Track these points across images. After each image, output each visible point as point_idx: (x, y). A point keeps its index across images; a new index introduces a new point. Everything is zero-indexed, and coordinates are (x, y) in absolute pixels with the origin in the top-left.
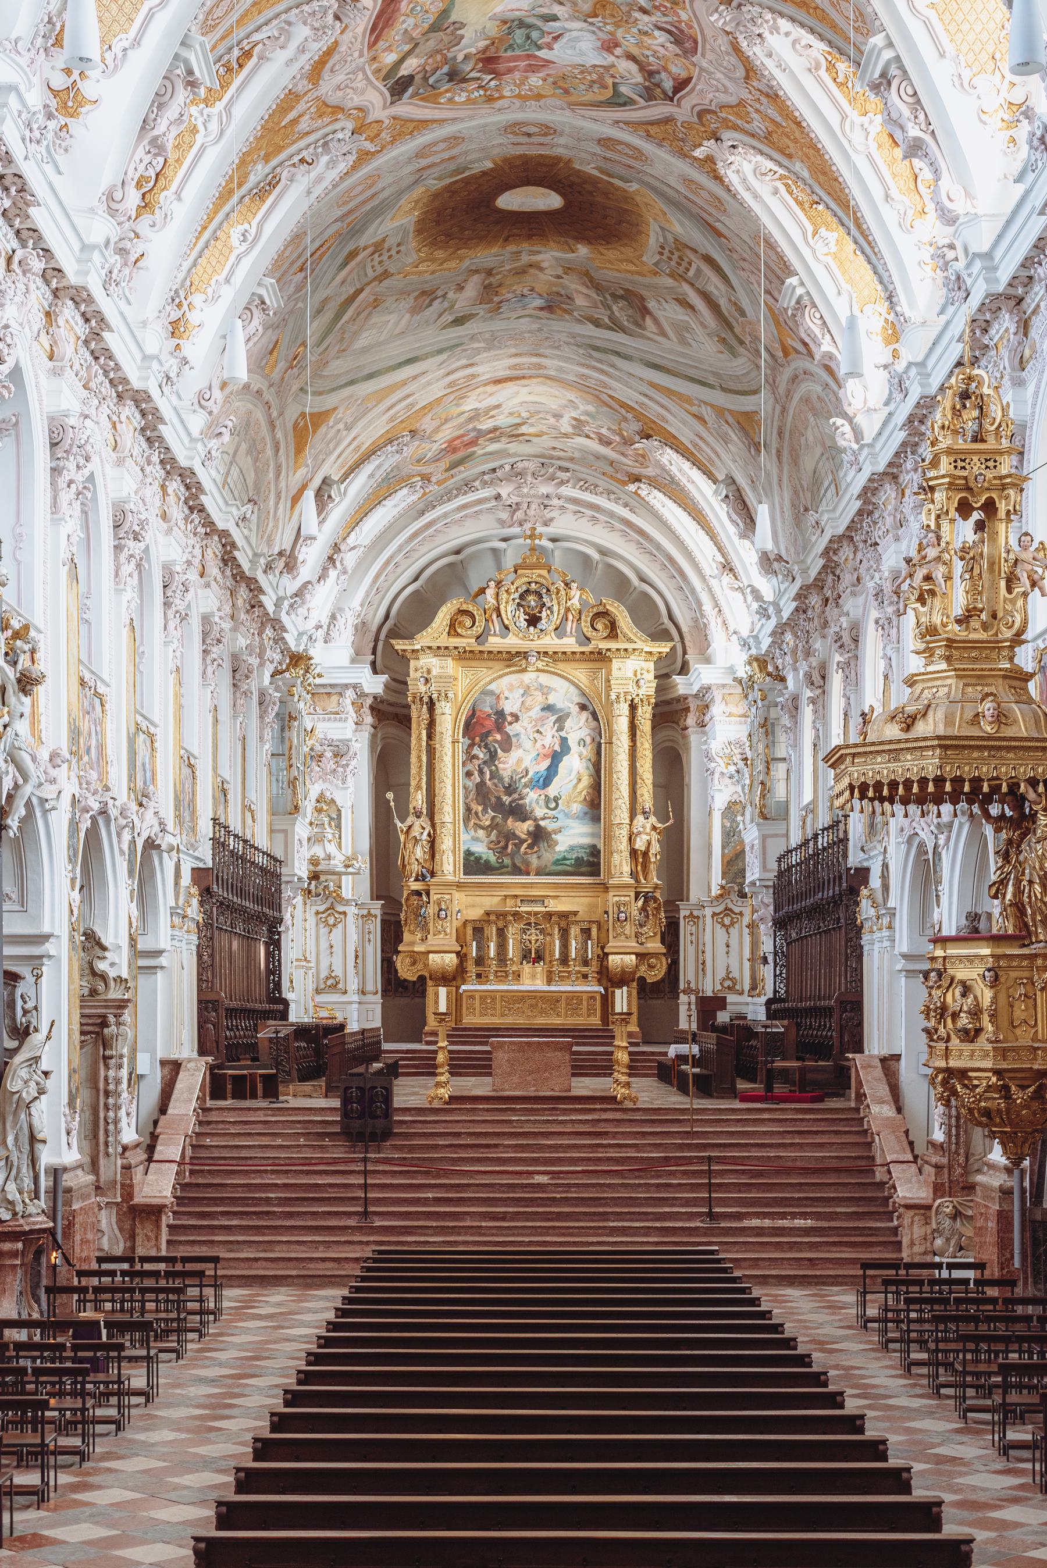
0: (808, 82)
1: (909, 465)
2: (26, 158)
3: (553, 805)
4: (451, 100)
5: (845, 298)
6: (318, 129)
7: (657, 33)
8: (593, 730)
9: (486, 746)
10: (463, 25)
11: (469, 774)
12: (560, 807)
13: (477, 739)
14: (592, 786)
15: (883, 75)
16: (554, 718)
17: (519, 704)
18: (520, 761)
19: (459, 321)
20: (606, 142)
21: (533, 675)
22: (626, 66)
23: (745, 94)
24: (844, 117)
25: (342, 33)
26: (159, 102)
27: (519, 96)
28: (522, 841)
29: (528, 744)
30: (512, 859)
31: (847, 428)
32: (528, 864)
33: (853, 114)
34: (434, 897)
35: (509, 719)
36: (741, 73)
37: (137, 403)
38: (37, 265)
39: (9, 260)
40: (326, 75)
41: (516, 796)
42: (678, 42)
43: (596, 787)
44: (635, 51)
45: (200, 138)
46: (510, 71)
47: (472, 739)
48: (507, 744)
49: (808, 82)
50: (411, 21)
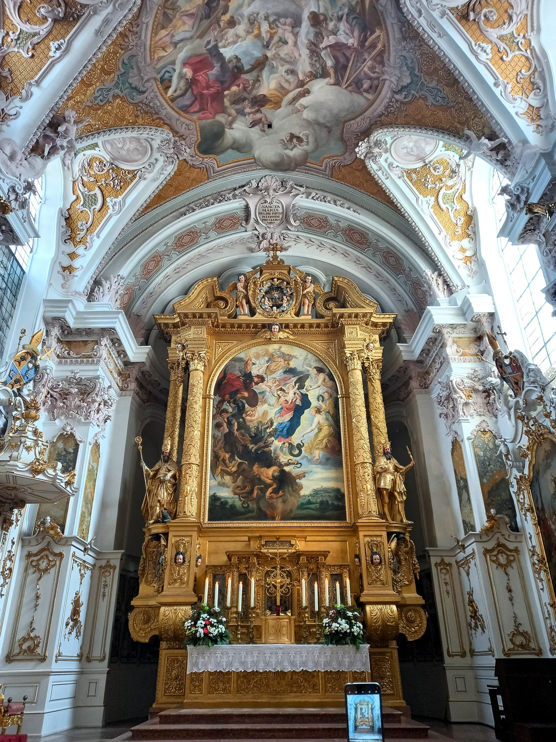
3: (297, 452)
8: (331, 388)
9: (235, 402)
11: (217, 426)
12: (303, 453)
13: (227, 396)
14: (330, 435)
16: (295, 379)
17: (264, 368)
18: (265, 413)
21: (276, 346)
28: (268, 486)
29: (273, 400)
30: (258, 503)
32: (273, 507)
34: (172, 540)
35: (256, 380)
41: (261, 444)
43: (336, 435)
47: (223, 397)
48: (254, 400)
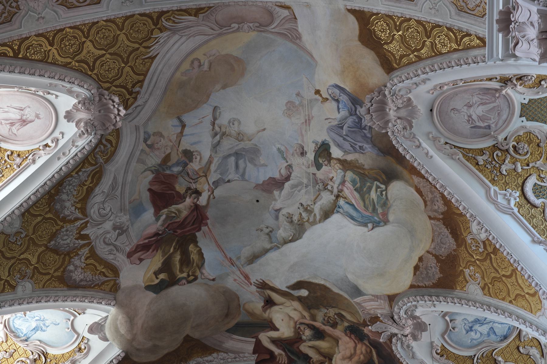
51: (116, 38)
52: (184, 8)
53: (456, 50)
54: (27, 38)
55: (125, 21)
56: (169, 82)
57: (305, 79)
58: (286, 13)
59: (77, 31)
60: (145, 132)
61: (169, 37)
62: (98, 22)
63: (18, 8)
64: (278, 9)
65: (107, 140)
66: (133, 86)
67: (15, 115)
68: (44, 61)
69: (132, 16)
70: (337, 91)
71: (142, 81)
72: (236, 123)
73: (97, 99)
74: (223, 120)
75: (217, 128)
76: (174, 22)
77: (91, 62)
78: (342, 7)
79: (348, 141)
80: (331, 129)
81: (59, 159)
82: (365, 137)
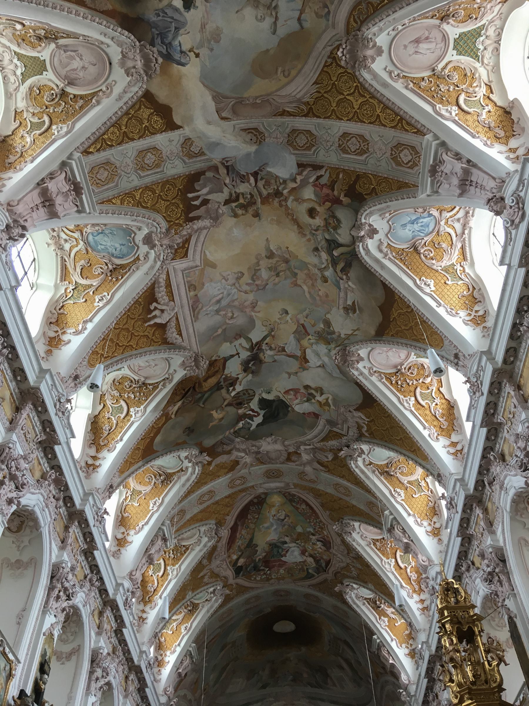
0: (368, 549)
1: (431, 698)
2: (94, 526)
4: (255, 578)
5: (394, 642)
6: (211, 583)
7: (318, 543)
10: (257, 546)
15: (391, 525)
19: (264, 687)
20: (307, 596)
22: (310, 560)
23: (349, 561)
24: (382, 560)
25: (218, 542)
26: (152, 542)
27: (277, 578)
31: (404, 693)
33: (384, 559)
36: (346, 552)
37: (136, 673)
38: (97, 584)
39: (85, 577)
40: (213, 560)
42: (324, 545)
44: (312, 553)
45: (170, 577)
46: (273, 567)
49: (368, 549)
50: (240, 542)
51: (338, 105)
52: (292, 117)
53: (104, 134)
54: (392, 127)
55: (330, 116)
56: (306, 62)
57: (208, 64)
58: (224, 115)
59: (361, 119)
60: (328, 20)
61: (303, 97)
62: (347, 120)
63: (392, 150)
64: (230, 117)
65: (356, 23)
66: (332, 63)
67: (423, 46)
68: (386, 107)
69: (325, 118)
70: (183, 61)
71: (325, 66)
72: (259, 17)
73: (356, 66)
74: (269, 21)
75: (274, 14)
76: (299, 108)
77: (356, 94)
78: (186, 128)
79: (169, 17)
80: (184, 24)
81: (394, 19)
82: (156, 27)
